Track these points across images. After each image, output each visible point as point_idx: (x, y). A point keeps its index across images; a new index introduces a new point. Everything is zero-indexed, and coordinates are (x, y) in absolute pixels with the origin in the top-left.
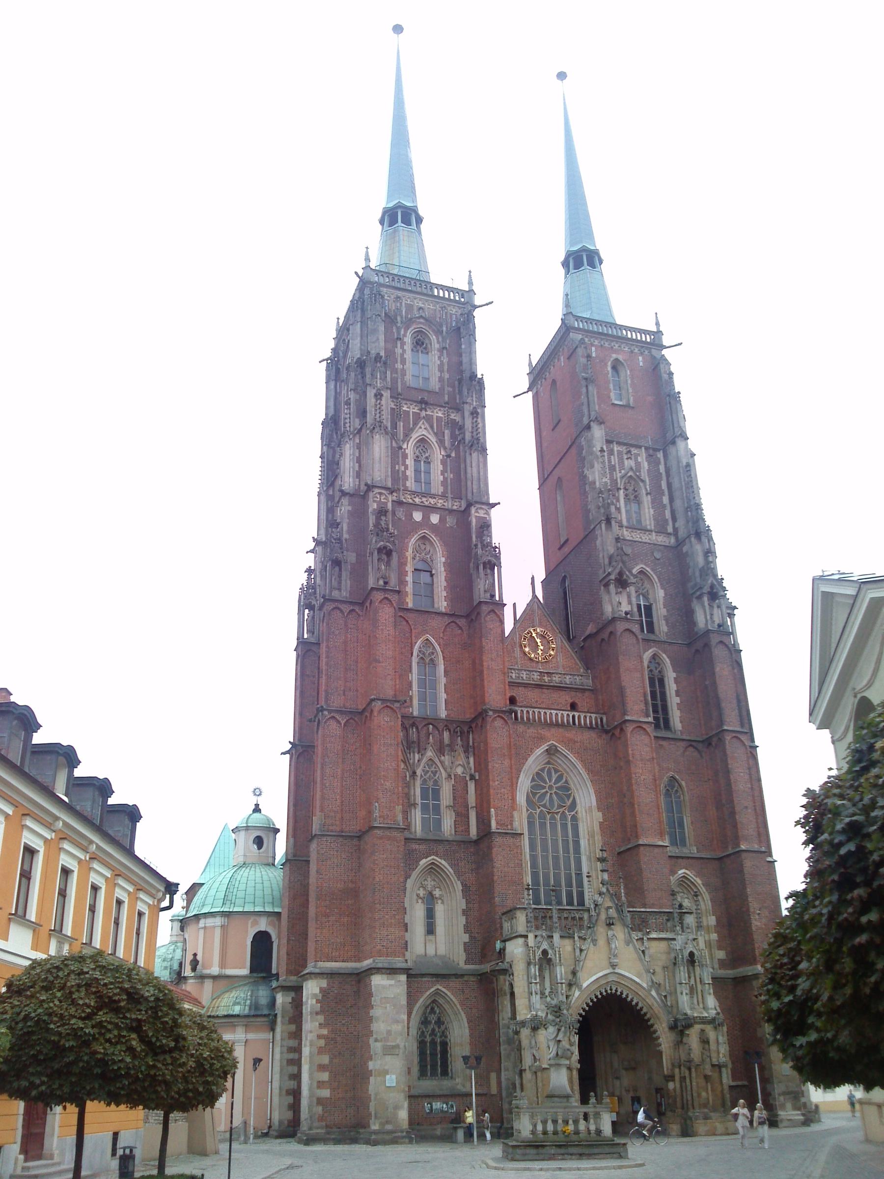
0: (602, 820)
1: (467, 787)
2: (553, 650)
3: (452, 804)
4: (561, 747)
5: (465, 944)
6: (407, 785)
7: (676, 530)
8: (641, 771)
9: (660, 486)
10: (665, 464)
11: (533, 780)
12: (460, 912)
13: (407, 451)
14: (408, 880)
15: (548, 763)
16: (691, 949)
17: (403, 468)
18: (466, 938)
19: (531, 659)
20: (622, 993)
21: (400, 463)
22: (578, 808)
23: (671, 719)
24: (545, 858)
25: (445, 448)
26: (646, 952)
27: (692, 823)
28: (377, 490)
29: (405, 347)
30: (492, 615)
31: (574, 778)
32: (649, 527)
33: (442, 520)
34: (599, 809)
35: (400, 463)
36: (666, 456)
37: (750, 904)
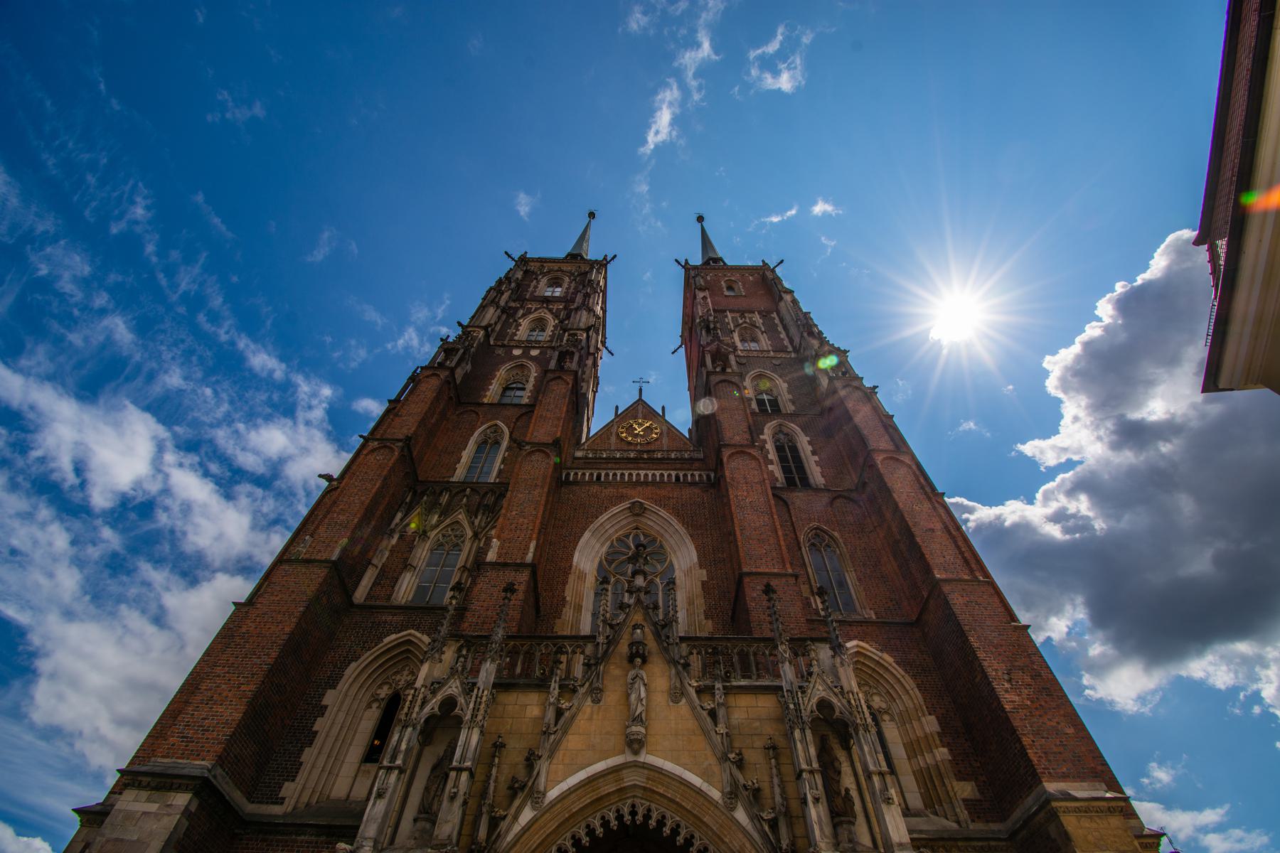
0: (705, 579)
2: (656, 434)
3: (468, 566)
4: (647, 504)
6: (411, 548)
7: (794, 348)
8: (745, 493)
14: (353, 665)
15: (637, 528)
16: (824, 694)
19: (629, 443)
20: (661, 823)
23: (810, 477)
25: (559, 319)
26: (721, 713)
27: (860, 580)
30: (559, 381)
31: (670, 539)
32: (766, 349)
36: (778, 314)
37: (985, 664)
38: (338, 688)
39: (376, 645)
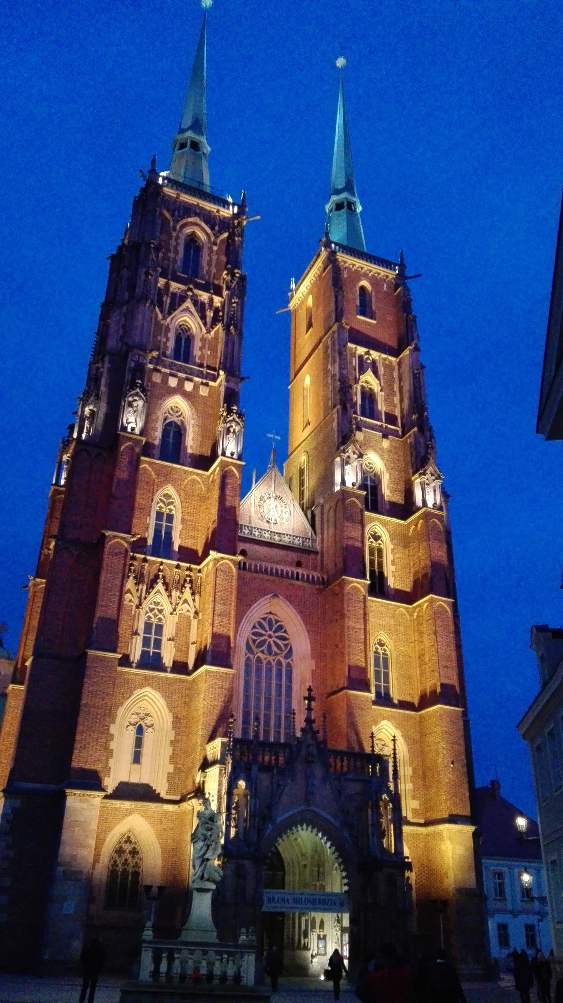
0: (314, 668)
1: (190, 625)
5: (169, 774)
9: (393, 388)
10: (399, 370)
11: (254, 627)
12: (168, 743)
13: (170, 326)
14: (120, 708)
17: (164, 340)
18: (171, 769)
21: (163, 335)
22: (295, 656)
24: (258, 699)
28: (136, 351)
29: (179, 241)
33: (196, 387)
34: (313, 657)
35: (163, 335)
38: (116, 723)
39: (130, 696)
